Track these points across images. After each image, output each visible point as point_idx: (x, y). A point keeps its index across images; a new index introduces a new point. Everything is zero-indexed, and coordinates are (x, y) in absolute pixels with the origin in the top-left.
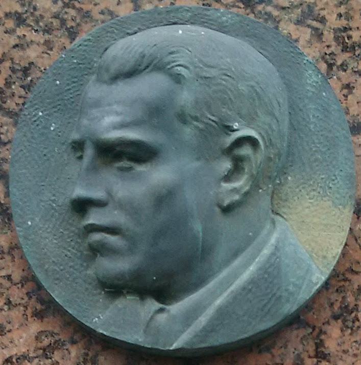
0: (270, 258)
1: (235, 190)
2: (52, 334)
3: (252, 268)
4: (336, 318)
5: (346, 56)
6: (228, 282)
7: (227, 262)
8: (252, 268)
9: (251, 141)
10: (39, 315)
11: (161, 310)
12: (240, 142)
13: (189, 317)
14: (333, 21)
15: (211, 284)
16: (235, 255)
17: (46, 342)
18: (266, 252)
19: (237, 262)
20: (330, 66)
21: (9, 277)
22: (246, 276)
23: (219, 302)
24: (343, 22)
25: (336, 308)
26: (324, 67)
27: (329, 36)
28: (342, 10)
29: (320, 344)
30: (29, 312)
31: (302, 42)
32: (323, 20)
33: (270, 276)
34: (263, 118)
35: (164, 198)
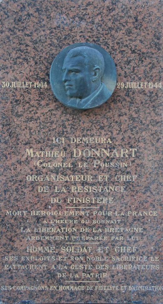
0: (102, 90)
1: (96, 78)
2: (58, 105)
3: (98, 92)
4: (113, 101)
5: (114, 52)
6: (93, 95)
7: (93, 92)
8: (98, 92)
9: (98, 69)
10: (55, 102)
11: (81, 101)
12: (97, 69)
13: (86, 102)
14: (111, 45)
15: (91, 95)
16: (95, 90)
17: (57, 107)
18: (101, 89)
19: (96, 91)
20: (111, 53)
21: (49, 94)
22: (97, 94)
23: (92, 99)
24: (113, 45)
25: (113, 99)
26: (109, 53)
27: (110, 48)
28: (113, 43)
29: (110, 107)
30: (53, 101)
31: (105, 49)
32: (109, 45)
33: (101, 95)
34: (101, 64)
35: (82, 79)
